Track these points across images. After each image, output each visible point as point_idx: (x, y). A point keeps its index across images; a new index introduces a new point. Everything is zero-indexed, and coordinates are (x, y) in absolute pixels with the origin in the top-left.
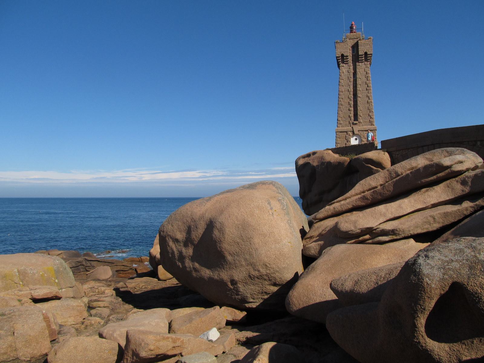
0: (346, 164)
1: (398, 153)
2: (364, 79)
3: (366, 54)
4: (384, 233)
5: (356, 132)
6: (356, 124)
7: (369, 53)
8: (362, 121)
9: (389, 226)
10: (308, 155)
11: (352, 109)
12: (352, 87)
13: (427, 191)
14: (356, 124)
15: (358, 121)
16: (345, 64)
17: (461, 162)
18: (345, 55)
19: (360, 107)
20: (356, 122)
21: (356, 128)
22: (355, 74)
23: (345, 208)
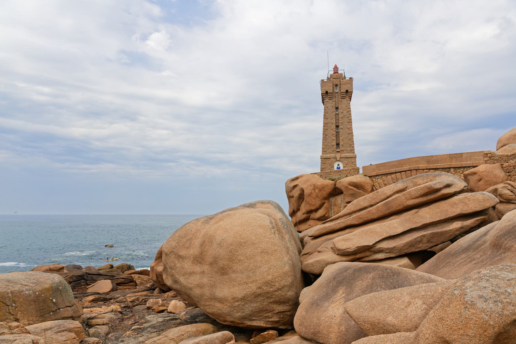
0: (332, 187)
1: (377, 177)
3: (347, 91)
4: (381, 251)
5: (338, 159)
9: (384, 245)
10: (297, 178)
13: (416, 212)
17: (448, 186)
18: (329, 92)
21: (338, 156)
23: (338, 227)
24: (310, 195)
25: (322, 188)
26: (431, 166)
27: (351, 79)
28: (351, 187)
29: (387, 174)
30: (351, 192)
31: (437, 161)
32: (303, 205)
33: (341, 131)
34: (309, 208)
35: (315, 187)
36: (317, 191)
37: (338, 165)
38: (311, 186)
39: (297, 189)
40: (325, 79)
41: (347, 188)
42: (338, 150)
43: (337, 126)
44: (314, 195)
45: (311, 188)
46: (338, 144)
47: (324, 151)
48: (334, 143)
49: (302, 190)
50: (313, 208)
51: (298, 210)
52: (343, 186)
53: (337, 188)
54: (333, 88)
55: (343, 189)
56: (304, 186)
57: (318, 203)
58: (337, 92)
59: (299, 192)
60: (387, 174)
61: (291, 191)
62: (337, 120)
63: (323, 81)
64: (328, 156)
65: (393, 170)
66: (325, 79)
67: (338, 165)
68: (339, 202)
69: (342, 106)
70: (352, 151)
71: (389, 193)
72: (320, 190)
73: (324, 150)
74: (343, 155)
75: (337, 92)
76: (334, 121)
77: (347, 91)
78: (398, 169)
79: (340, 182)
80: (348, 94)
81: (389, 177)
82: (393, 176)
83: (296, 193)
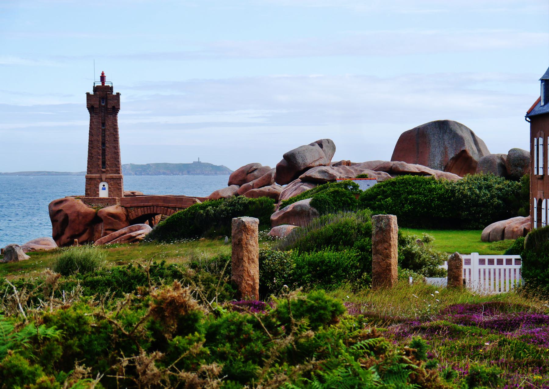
2: (112, 131)
3: (114, 107)
5: (104, 179)
6: (104, 172)
7: (116, 107)
8: (108, 169)
10: (61, 202)
11: (101, 157)
12: (100, 137)
14: (104, 172)
15: (105, 168)
16: (96, 114)
19: (108, 157)
20: (103, 170)
21: (104, 176)
22: (104, 124)
24: (74, 221)
27: (118, 94)
28: (109, 217)
29: (138, 207)
30: (110, 221)
33: (107, 149)
36: (80, 218)
37: (104, 186)
38: (75, 212)
39: (62, 213)
40: (92, 92)
41: (106, 217)
42: (103, 170)
43: (104, 144)
45: (75, 215)
46: (104, 163)
47: (89, 171)
48: (100, 163)
49: (66, 216)
52: (103, 215)
54: (100, 102)
55: (102, 217)
56: (68, 212)
57: (82, 228)
58: (103, 104)
62: (104, 137)
63: (88, 94)
64: (94, 175)
65: (142, 204)
66: (92, 92)
67: (104, 186)
68: (100, 228)
69: (109, 123)
70: (118, 171)
71: (117, 235)
72: (83, 217)
73: (90, 169)
74: (109, 175)
75: (103, 104)
76: (100, 138)
77: (114, 107)
79: (101, 211)
80: (116, 109)
82: (142, 209)
83: (60, 218)
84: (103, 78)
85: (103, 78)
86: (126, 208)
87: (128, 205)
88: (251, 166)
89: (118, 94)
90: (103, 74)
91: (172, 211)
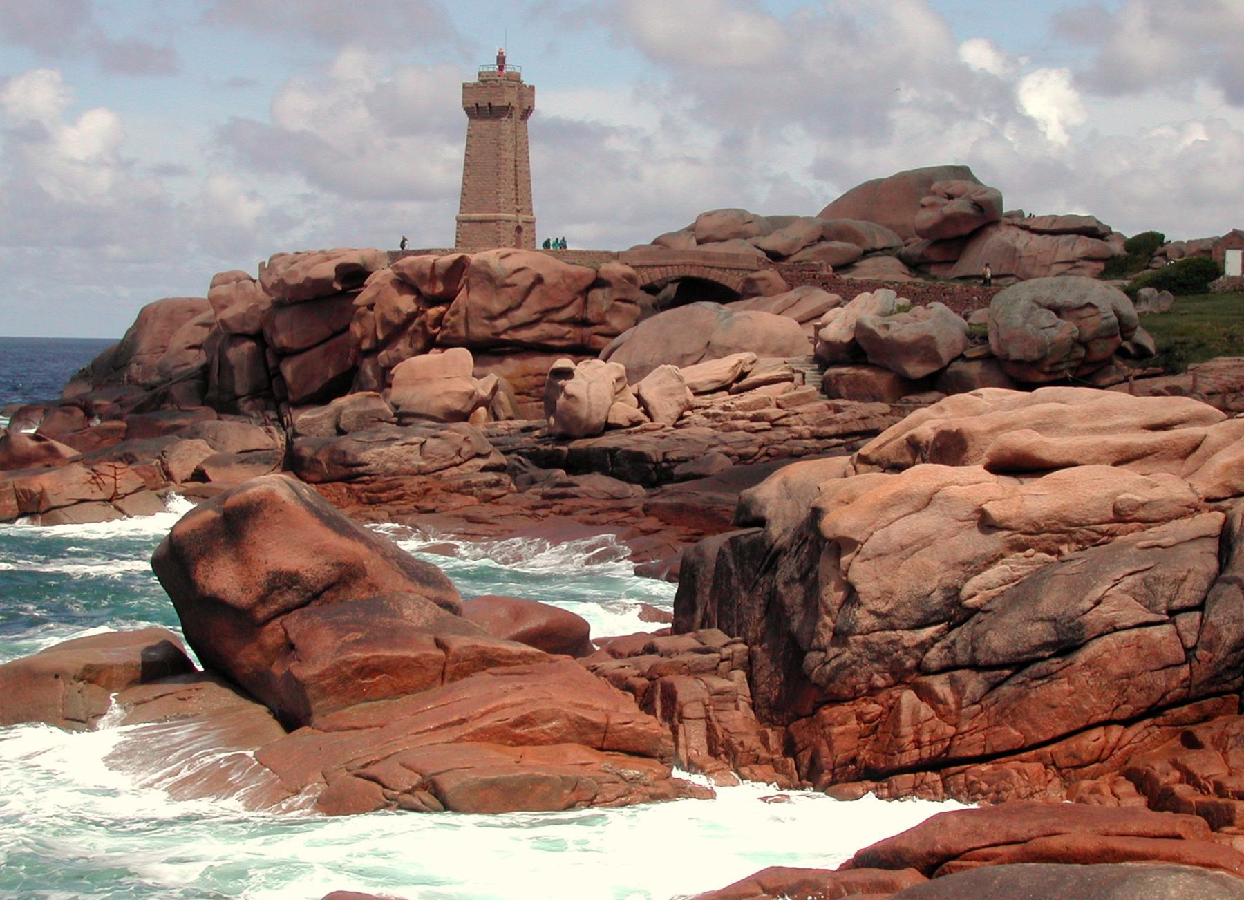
0: (593, 277)
24: (555, 286)
25: (577, 278)
26: (707, 263)
27: (532, 88)
29: (654, 266)
30: (624, 286)
31: (714, 259)
32: (532, 299)
34: (548, 304)
35: (565, 275)
36: (569, 281)
38: (556, 272)
41: (619, 280)
44: (563, 286)
50: (558, 305)
51: (519, 306)
53: (601, 279)
55: (613, 281)
56: (541, 271)
57: (567, 297)
59: (532, 280)
60: (654, 266)
61: (509, 276)
78: (670, 262)
79: (607, 272)
81: (656, 269)
84: (501, 60)
85: (501, 60)
86: (633, 267)
87: (637, 263)
88: (742, 213)
89: (532, 88)
90: (501, 53)
91: (720, 273)
